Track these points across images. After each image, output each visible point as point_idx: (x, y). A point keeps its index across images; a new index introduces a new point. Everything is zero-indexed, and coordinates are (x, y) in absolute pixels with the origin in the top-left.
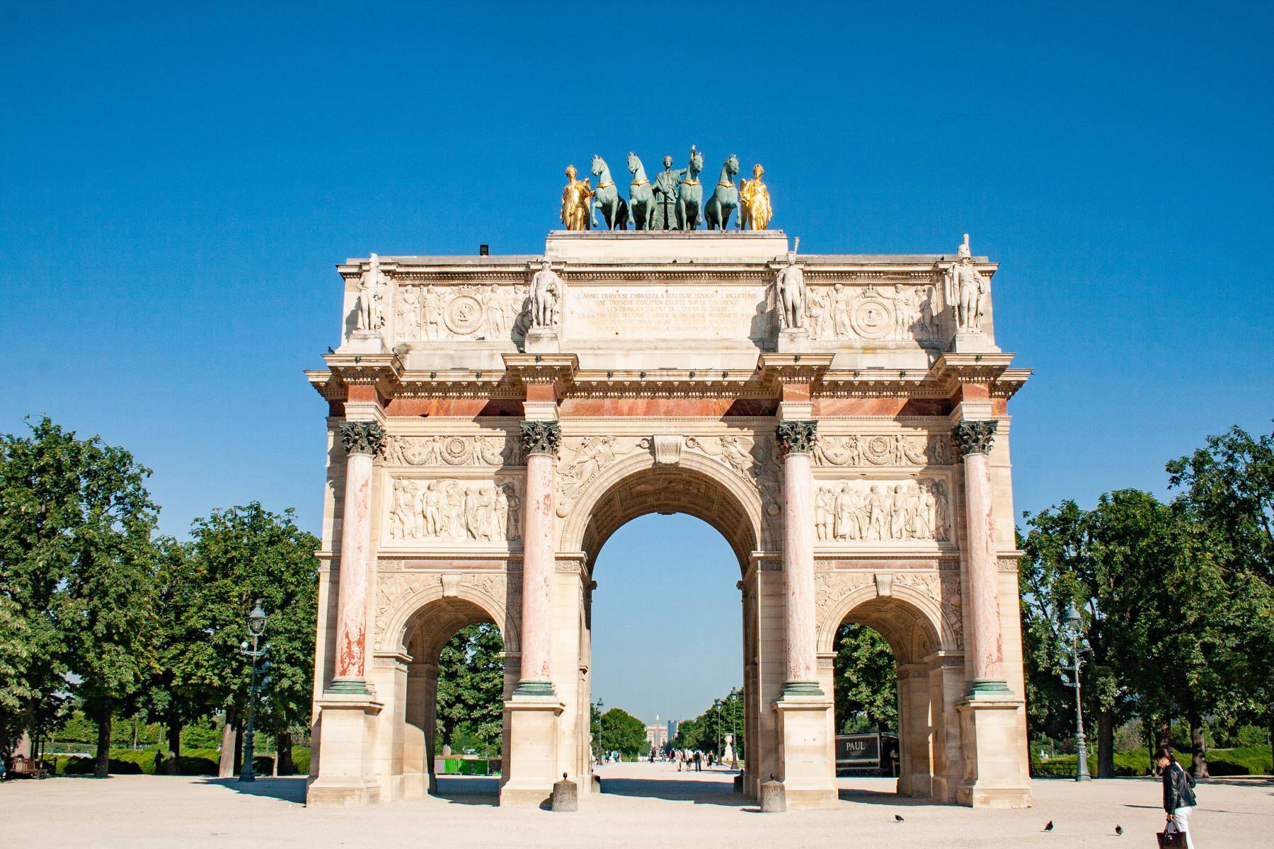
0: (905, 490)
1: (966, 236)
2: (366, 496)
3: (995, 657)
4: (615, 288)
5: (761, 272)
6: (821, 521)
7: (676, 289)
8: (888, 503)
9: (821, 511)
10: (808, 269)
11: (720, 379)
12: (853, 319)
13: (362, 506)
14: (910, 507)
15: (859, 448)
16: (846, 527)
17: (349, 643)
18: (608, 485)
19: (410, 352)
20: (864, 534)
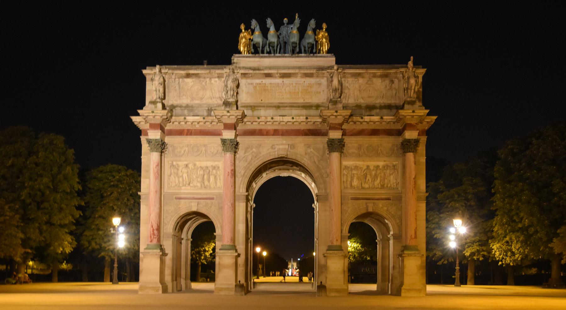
0: (381, 167)
1: (412, 57)
2: (158, 170)
4: (261, 80)
5: (324, 73)
6: (345, 180)
7: (287, 81)
8: (373, 173)
9: (345, 176)
10: (343, 72)
13: (157, 174)
14: (383, 174)
15: (362, 150)
17: (153, 230)
18: (257, 165)
19: (176, 108)
20: (363, 185)
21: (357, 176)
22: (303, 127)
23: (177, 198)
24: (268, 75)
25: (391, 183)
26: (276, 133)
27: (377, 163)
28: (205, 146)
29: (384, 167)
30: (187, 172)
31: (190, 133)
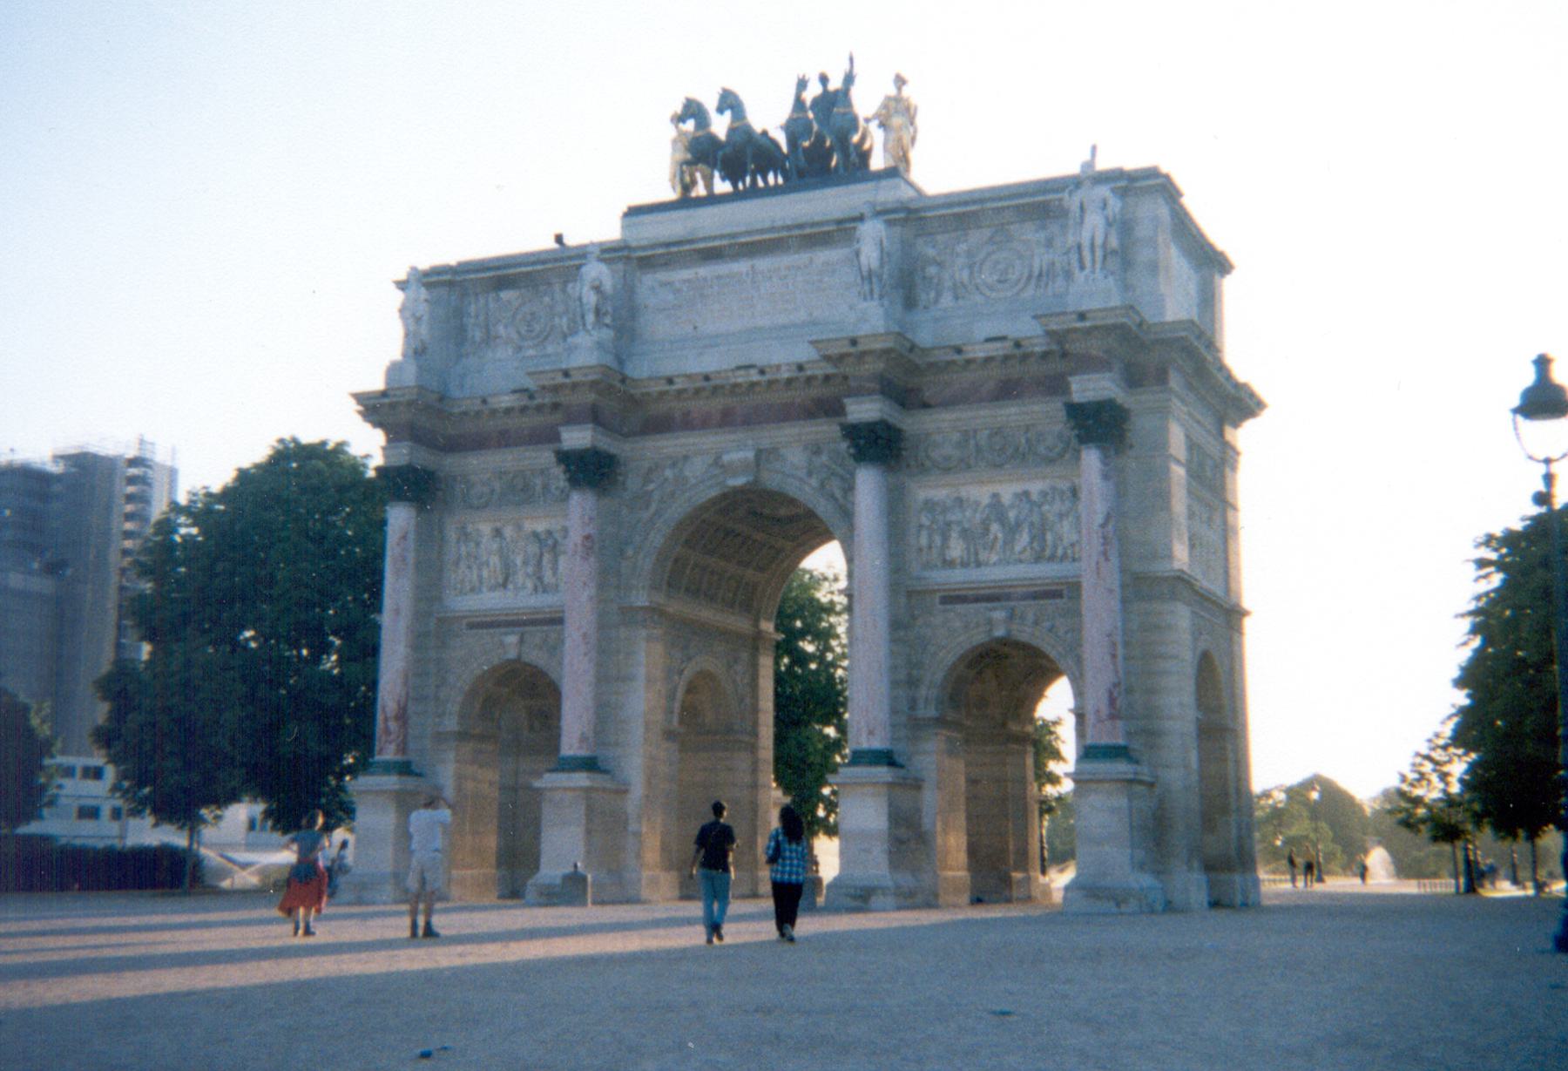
0: (1035, 497)
3: (1105, 710)
6: (924, 541)
7: (764, 263)
11: (795, 374)
12: (976, 275)
14: (1035, 518)
16: (956, 549)
17: (386, 720)
21: (959, 529)
22: (799, 396)
23: (471, 626)
24: (712, 255)
25: (1066, 542)
26: (726, 420)
27: (1018, 487)
28: (542, 472)
29: (1044, 494)
30: (501, 549)
31: (505, 440)
